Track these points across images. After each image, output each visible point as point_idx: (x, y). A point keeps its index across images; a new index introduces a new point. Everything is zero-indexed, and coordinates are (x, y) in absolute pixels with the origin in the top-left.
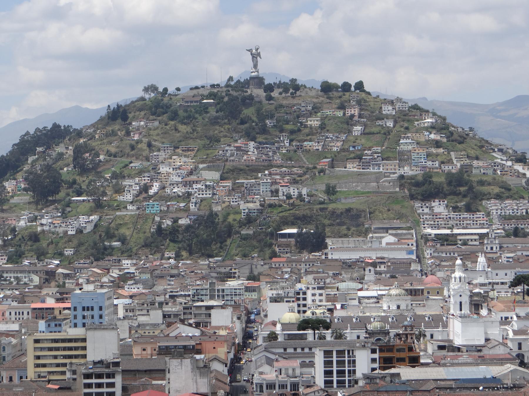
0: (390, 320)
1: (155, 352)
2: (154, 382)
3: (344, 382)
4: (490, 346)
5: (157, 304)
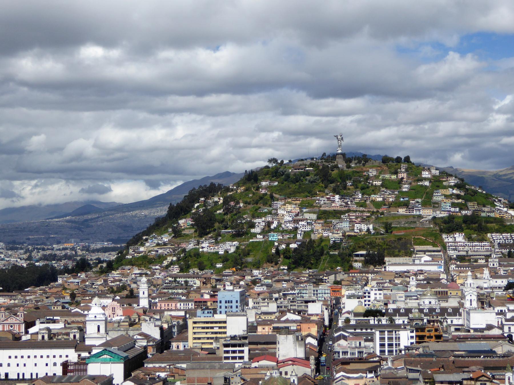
5: (274, 299)
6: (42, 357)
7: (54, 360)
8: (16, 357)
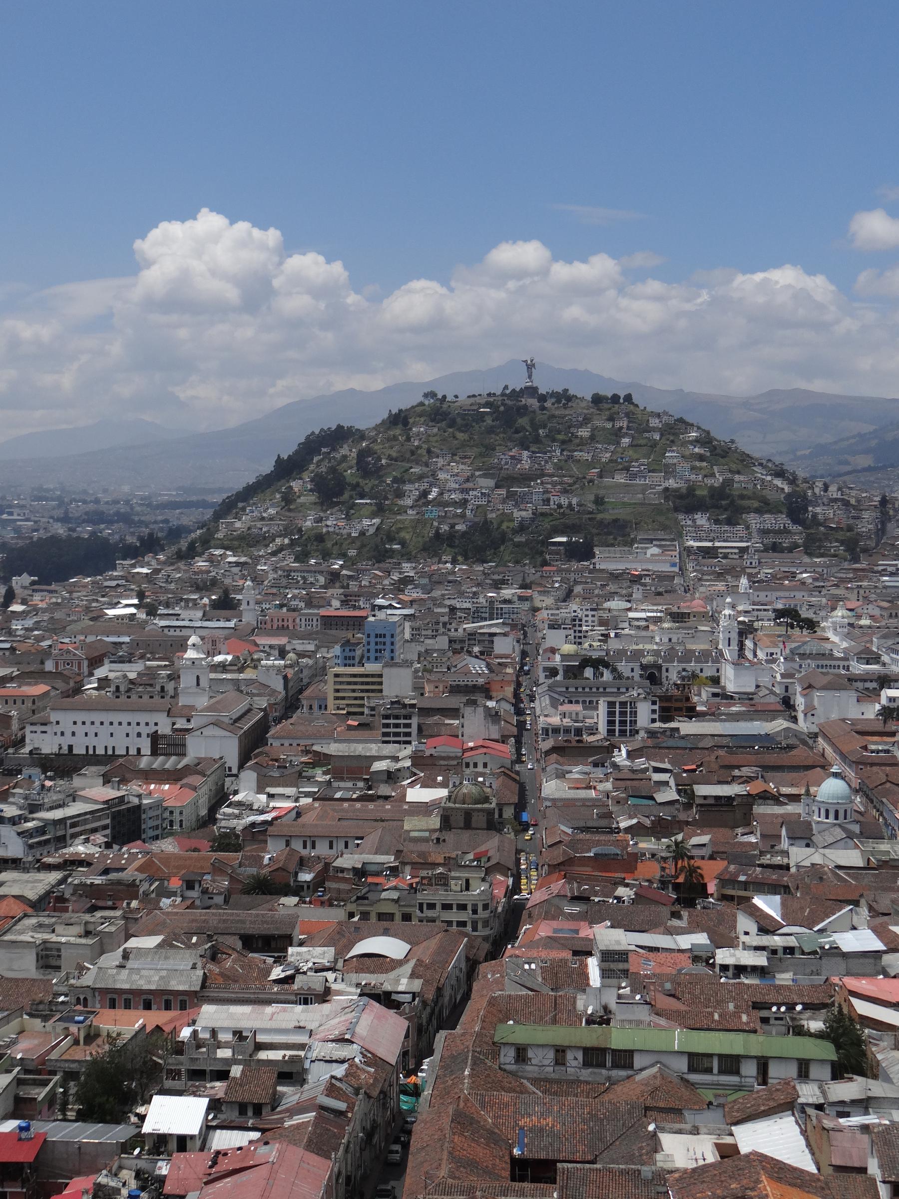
2: (447, 721)
4: (761, 694)
6: (120, 724)
8: (84, 723)
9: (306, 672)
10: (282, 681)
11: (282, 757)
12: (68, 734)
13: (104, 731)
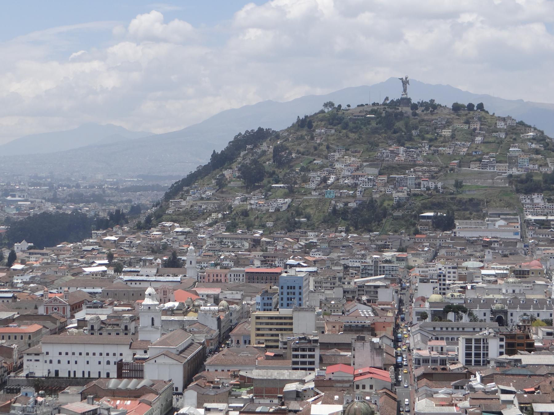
0: (508, 302)
1: (341, 329)
2: (342, 353)
3: (479, 361)
5: (337, 279)
6: (94, 354)
7: (107, 358)
8: (67, 354)
9: (234, 316)
10: (216, 322)
11: (216, 380)
12: (55, 362)
13: (82, 360)
